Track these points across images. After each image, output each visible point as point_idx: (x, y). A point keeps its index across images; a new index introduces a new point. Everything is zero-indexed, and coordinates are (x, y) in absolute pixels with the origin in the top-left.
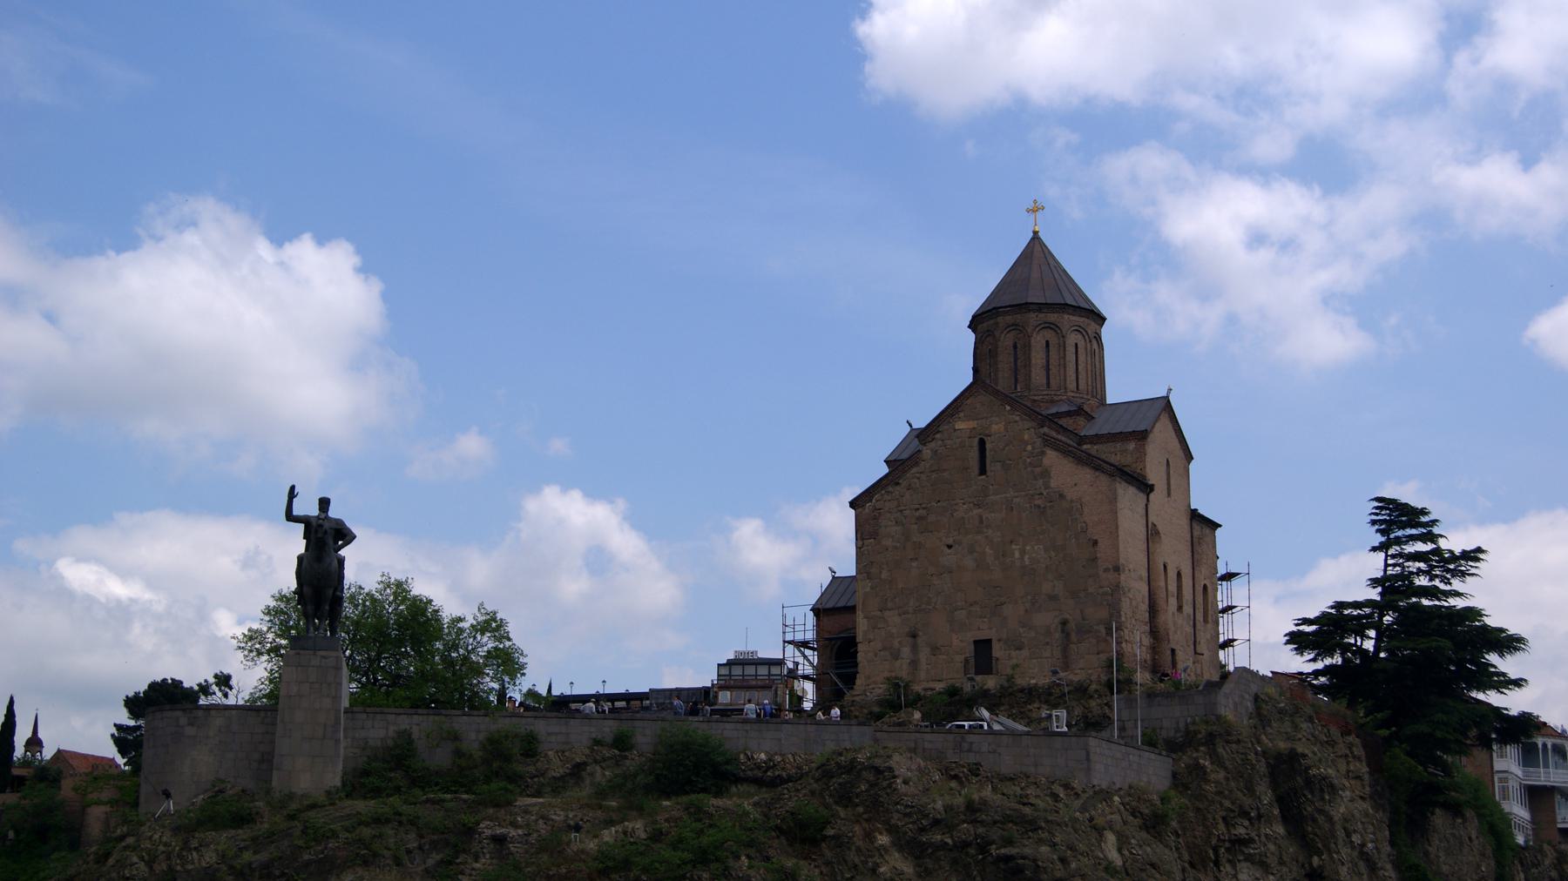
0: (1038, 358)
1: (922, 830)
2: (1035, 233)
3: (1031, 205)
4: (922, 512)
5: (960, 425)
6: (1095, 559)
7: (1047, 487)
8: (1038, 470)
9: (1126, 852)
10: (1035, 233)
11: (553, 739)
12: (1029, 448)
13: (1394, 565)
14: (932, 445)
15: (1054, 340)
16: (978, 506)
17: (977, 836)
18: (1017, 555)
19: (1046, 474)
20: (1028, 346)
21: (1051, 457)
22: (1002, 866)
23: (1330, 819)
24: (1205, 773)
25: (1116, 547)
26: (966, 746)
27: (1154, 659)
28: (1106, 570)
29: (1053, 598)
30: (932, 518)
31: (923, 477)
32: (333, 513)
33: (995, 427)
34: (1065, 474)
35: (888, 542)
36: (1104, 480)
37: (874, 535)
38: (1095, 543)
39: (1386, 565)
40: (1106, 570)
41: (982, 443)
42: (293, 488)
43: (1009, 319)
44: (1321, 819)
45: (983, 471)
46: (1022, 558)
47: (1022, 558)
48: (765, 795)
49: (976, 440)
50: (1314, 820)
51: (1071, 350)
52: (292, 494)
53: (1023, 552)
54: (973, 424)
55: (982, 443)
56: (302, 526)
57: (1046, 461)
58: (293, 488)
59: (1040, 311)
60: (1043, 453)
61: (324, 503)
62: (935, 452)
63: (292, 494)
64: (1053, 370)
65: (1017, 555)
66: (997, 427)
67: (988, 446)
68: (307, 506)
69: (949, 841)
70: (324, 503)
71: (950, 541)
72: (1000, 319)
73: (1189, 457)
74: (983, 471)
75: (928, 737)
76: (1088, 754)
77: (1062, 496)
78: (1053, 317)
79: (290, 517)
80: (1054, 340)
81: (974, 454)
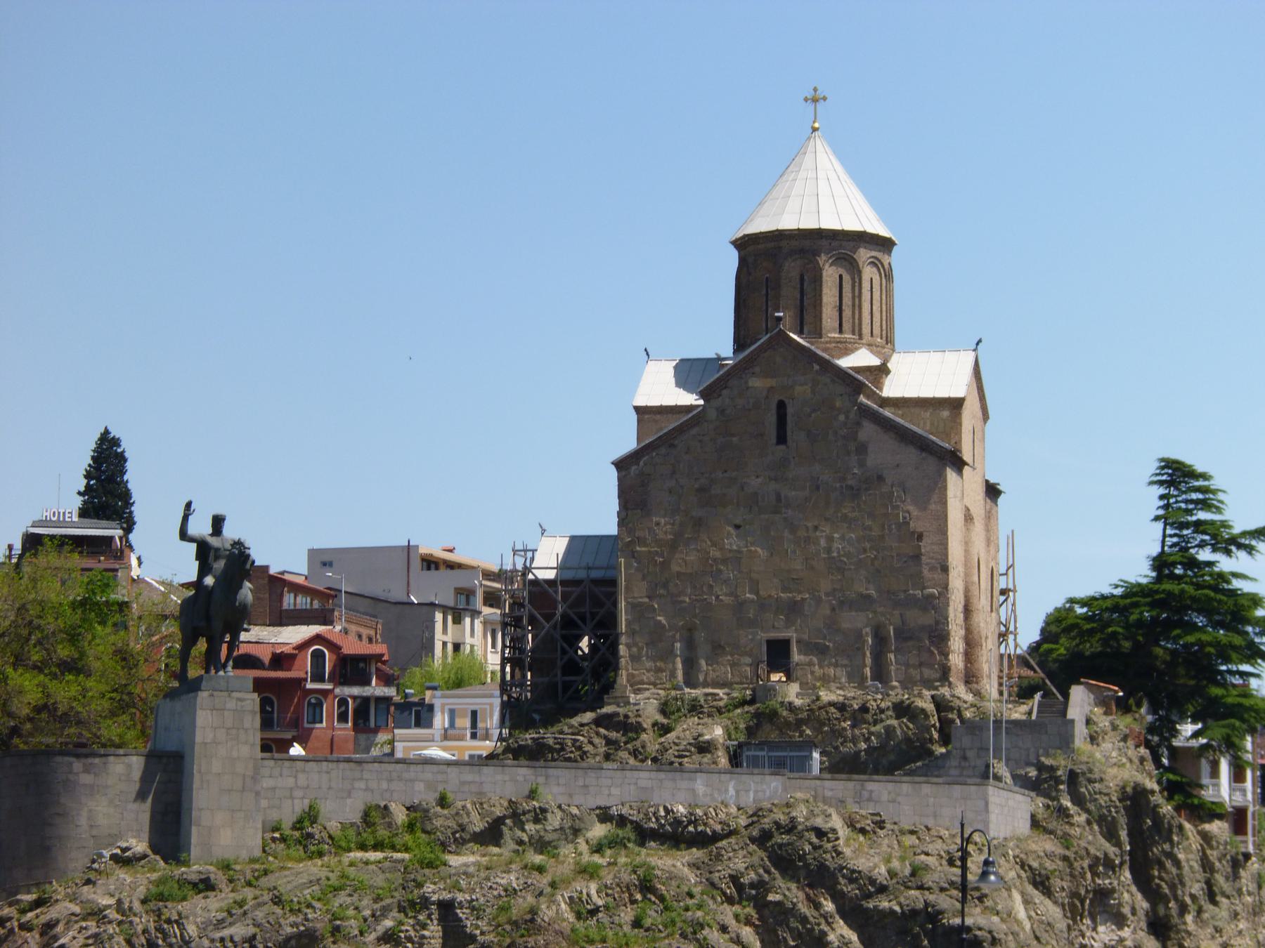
0: (829, 296)
1: (869, 896)
3: (810, 94)
6: (917, 557)
7: (862, 464)
9: (1033, 914)
11: (466, 788)
13: (1171, 536)
15: (846, 278)
16: (776, 479)
17: (927, 904)
18: (823, 542)
19: (862, 449)
20: (817, 280)
21: (868, 431)
23: (1177, 863)
24: (1069, 816)
26: (866, 794)
27: (966, 667)
28: (932, 569)
32: (231, 532)
33: (798, 389)
36: (932, 462)
39: (1164, 536)
41: (781, 406)
42: (189, 505)
44: (1168, 864)
45: (782, 439)
48: (696, 853)
49: (774, 406)
50: (1162, 866)
51: (866, 285)
53: (830, 539)
55: (781, 406)
56: (194, 546)
57: (862, 435)
58: (189, 505)
60: (858, 424)
61: (218, 522)
62: (721, 411)
64: (847, 313)
65: (823, 542)
66: (802, 390)
67: (790, 410)
68: (200, 526)
69: (897, 908)
70: (218, 522)
73: (986, 416)
74: (782, 439)
75: (827, 783)
76: (987, 804)
79: (184, 535)
81: (772, 418)
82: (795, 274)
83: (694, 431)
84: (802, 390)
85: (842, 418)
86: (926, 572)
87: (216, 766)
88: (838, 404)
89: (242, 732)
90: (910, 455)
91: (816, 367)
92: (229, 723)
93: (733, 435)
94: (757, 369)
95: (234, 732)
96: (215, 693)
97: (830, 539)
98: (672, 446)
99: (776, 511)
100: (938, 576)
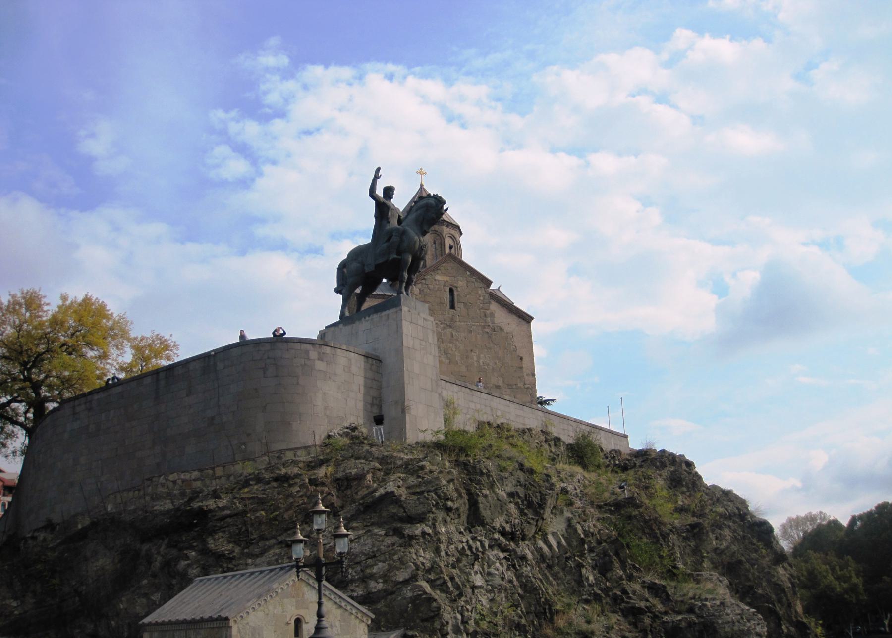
2: (422, 185)
5: (438, 277)
6: (521, 368)
10: (422, 185)
12: (481, 298)
16: (450, 327)
18: (475, 359)
19: (492, 315)
21: (494, 306)
22: (756, 528)
28: (528, 375)
38: (521, 359)
40: (528, 375)
42: (378, 169)
45: (452, 307)
52: (376, 177)
53: (479, 358)
54: (448, 278)
55: (451, 291)
58: (378, 169)
60: (490, 303)
61: (389, 192)
63: (376, 177)
66: (461, 283)
67: (456, 293)
74: (452, 307)
77: (501, 329)
78: (453, 232)
81: (447, 295)
95: (423, 343)
97: (479, 358)
99: (451, 343)
100: (531, 378)
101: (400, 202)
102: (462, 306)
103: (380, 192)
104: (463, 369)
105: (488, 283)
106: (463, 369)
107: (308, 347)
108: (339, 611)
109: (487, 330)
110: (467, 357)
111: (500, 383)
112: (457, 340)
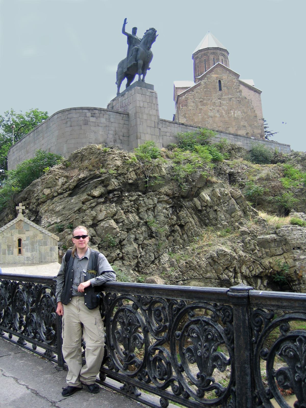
4: (201, 100)
5: (213, 76)
8: (238, 90)
12: (235, 84)
14: (204, 81)
19: (240, 91)
21: (242, 87)
25: (261, 113)
29: (244, 126)
30: (205, 102)
31: (201, 90)
33: (224, 77)
34: (245, 92)
35: (190, 108)
37: (186, 105)
40: (260, 119)
41: (220, 81)
42: (126, 19)
43: (212, 51)
45: (220, 89)
46: (234, 115)
47: (234, 115)
49: (218, 81)
52: (125, 23)
53: (234, 113)
54: (216, 76)
55: (220, 81)
58: (126, 19)
59: (220, 50)
61: (135, 30)
63: (125, 23)
67: (222, 82)
70: (135, 30)
71: (211, 108)
72: (209, 51)
74: (220, 89)
77: (245, 98)
78: (223, 53)
79: (124, 32)
80: (224, 59)
81: (218, 84)
82: (212, 58)
83: (198, 87)
84: (225, 77)
85: (235, 84)
86: (258, 120)
87: (145, 117)
88: (234, 81)
89: (153, 104)
90: (252, 93)
91: (228, 72)
92: (148, 101)
93: (208, 88)
94: (213, 73)
95: (150, 104)
96: (142, 88)
97: (234, 113)
98: (193, 91)
99: (220, 106)
101: (140, 35)
102: (226, 88)
103: (130, 32)
104: (227, 119)
105: (237, 76)
106: (227, 119)
107: (86, 111)
108: (42, 235)
109: (238, 99)
110: (229, 113)
111: (246, 124)
112: (223, 105)
